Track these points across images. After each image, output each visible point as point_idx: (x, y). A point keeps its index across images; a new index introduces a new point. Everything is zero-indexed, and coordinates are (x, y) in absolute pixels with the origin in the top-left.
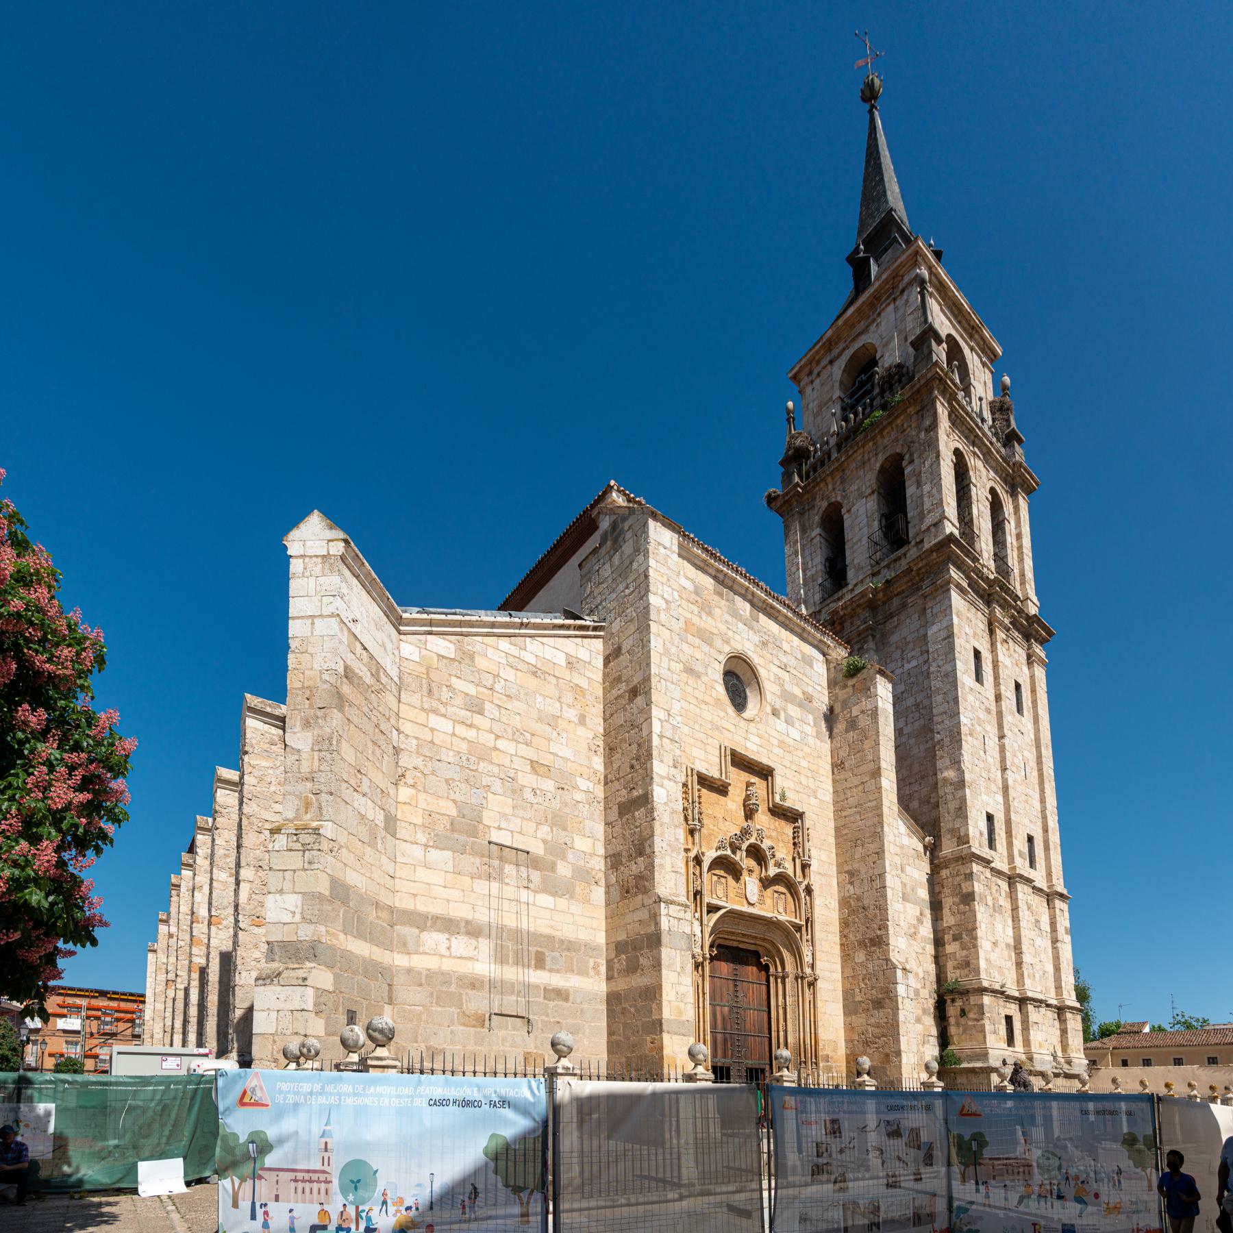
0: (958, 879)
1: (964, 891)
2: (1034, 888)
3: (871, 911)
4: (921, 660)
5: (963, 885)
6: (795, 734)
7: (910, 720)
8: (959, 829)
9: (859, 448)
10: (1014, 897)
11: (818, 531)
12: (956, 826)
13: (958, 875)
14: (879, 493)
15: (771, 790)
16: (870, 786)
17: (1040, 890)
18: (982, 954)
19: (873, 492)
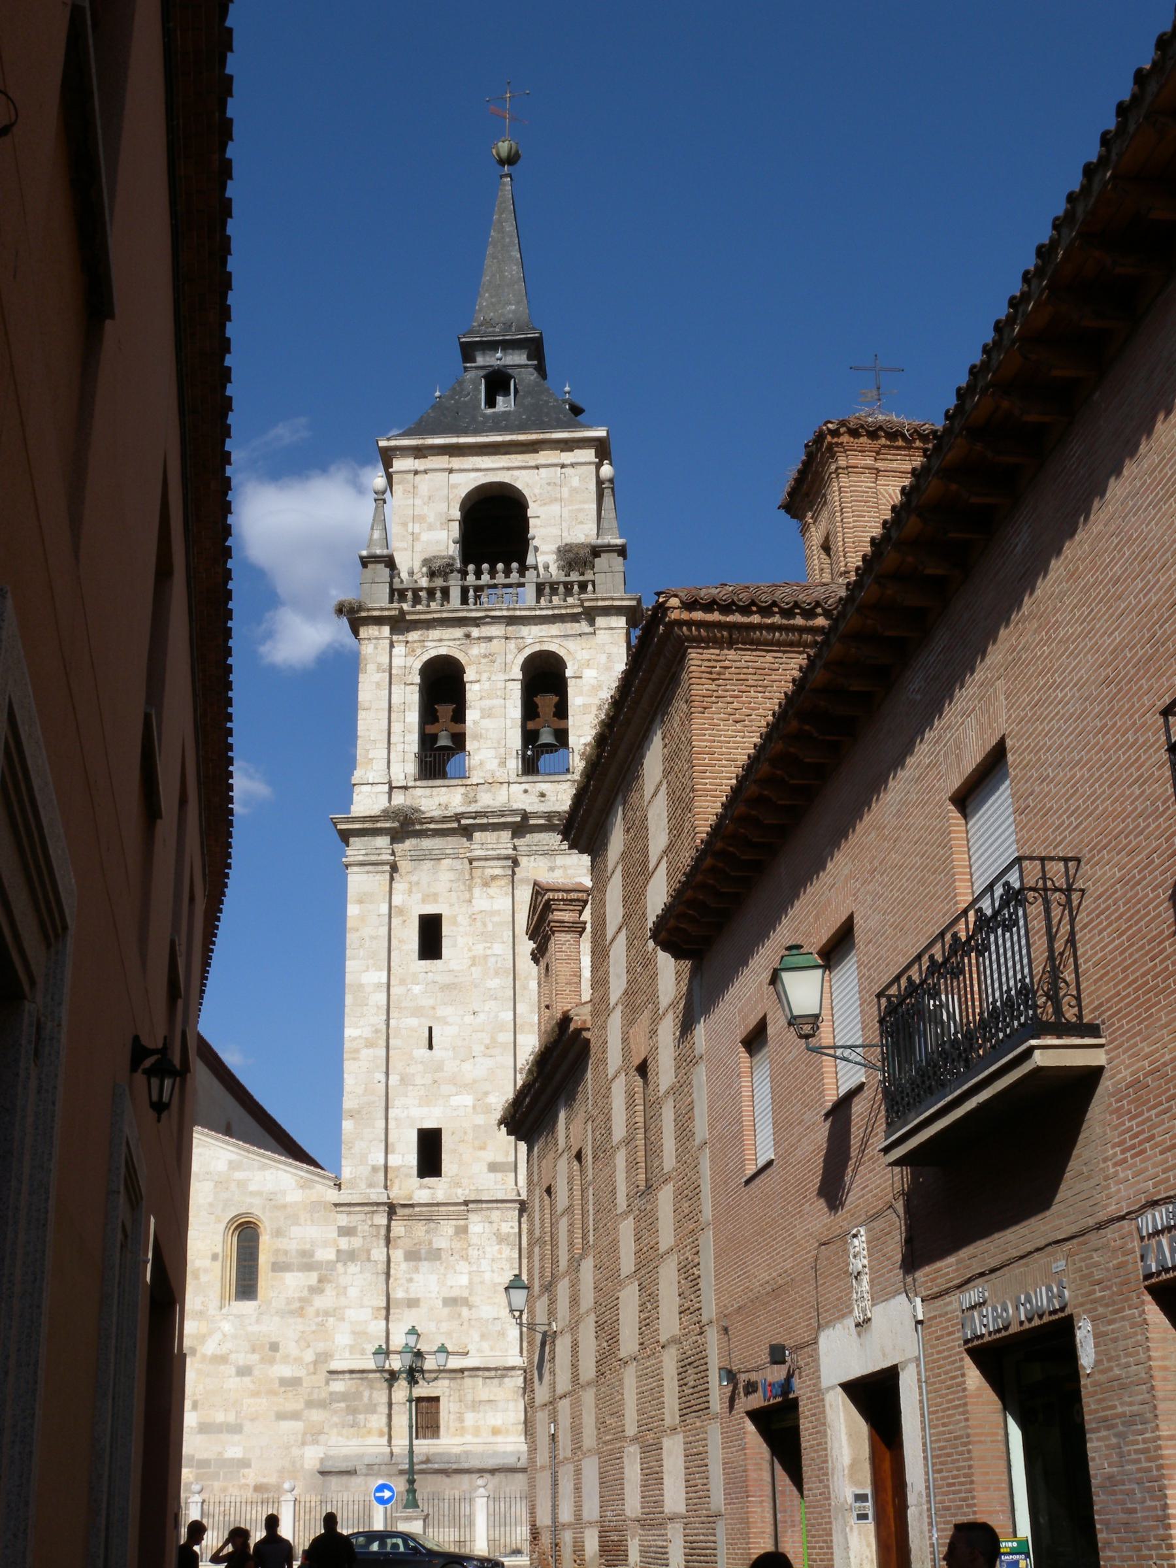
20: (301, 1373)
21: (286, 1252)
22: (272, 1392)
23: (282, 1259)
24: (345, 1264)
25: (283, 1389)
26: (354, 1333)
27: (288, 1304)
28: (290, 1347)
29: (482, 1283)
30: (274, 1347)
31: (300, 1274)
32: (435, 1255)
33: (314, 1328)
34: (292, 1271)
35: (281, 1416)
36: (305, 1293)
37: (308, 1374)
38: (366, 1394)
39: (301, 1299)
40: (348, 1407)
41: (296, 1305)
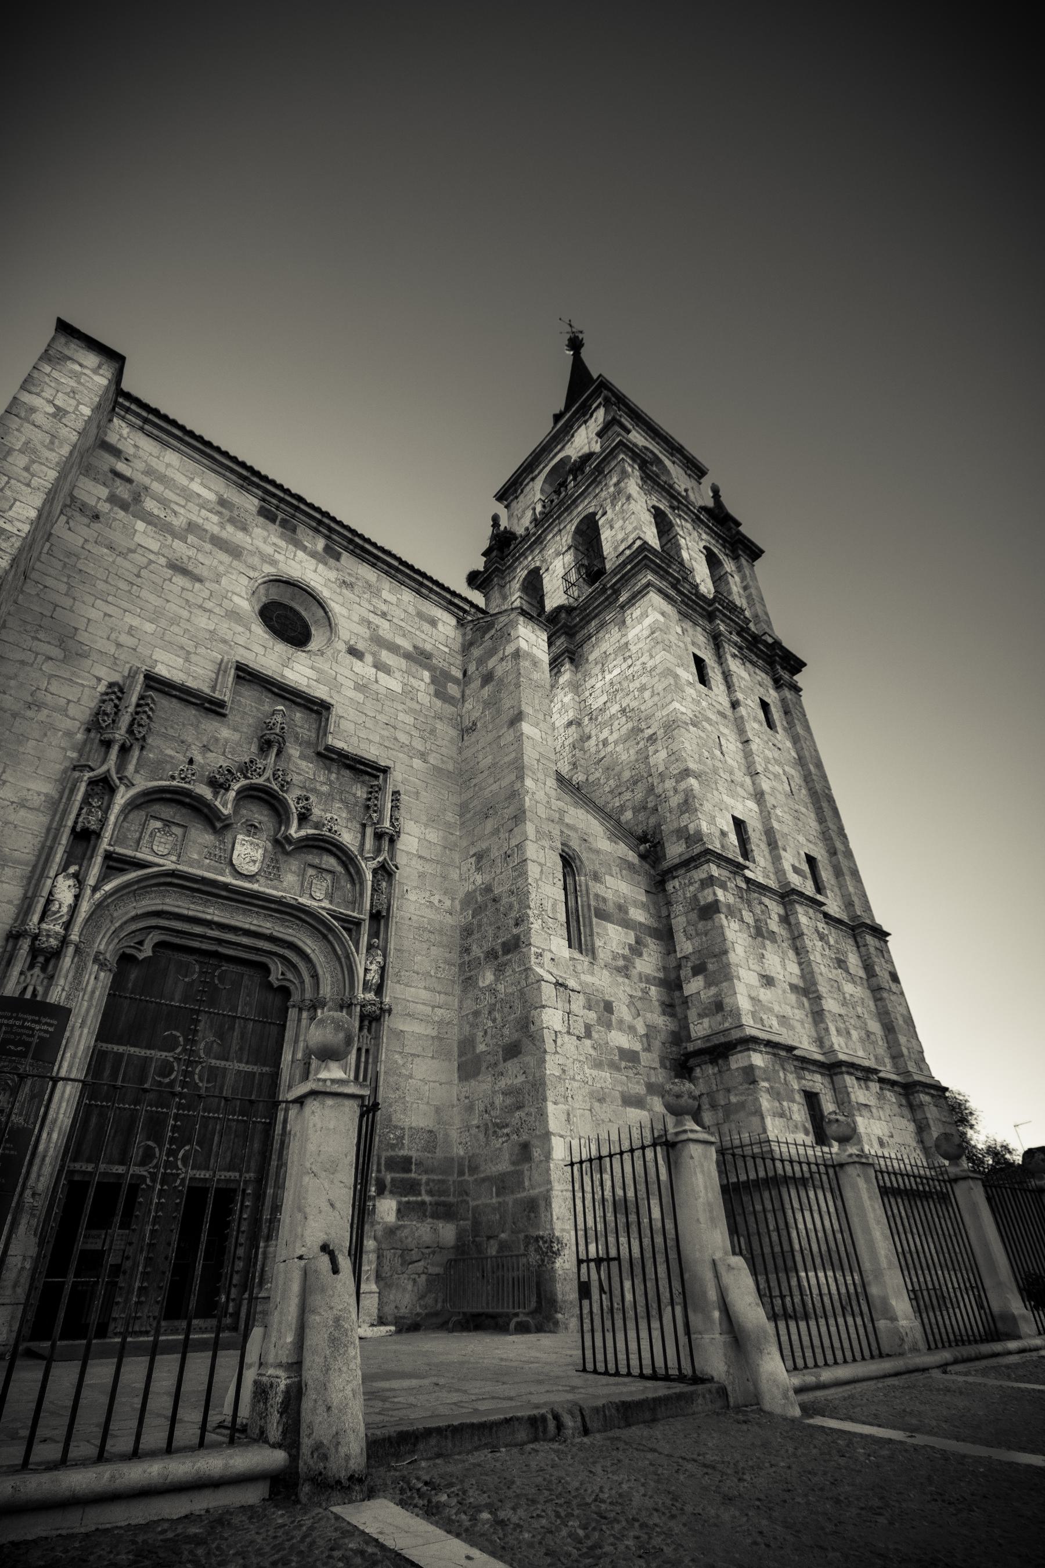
0: (692, 888)
1: (702, 903)
2: (826, 915)
3: (504, 901)
4: (624, 666)
5: (699, 895)
6: (393, 683)
7: (616, 726)
8: (686, 826)
9: (554, 520)
10: (793, 921)
11: (518, 594)
12: (682, 825)
13: (691, 884)
14: (576, 549)
15: (322, 730)
16: (509, 736)
17: (839, 921)
18: (740, 988)
19: (569, 548)
20: (637, 1047)
21: (604, 900)
22: (614, 1066)
23: (602, 906)
24: (726, 917)
25: (623, 1064)
26: (752, 998)
27: (614, 959)
28: (623, 1011)
29: (821, 974)
30: (608, 1007)
31: (620, 928)
32: (772, 936)
33: (640, 994)
34: (613, 923)
35: (630, 1101)
36: (627, 952)
37: (644, 1050)
38: (781, 1074)
39: (624, 957)
40: (772, 1087)
41: (621, 963)
